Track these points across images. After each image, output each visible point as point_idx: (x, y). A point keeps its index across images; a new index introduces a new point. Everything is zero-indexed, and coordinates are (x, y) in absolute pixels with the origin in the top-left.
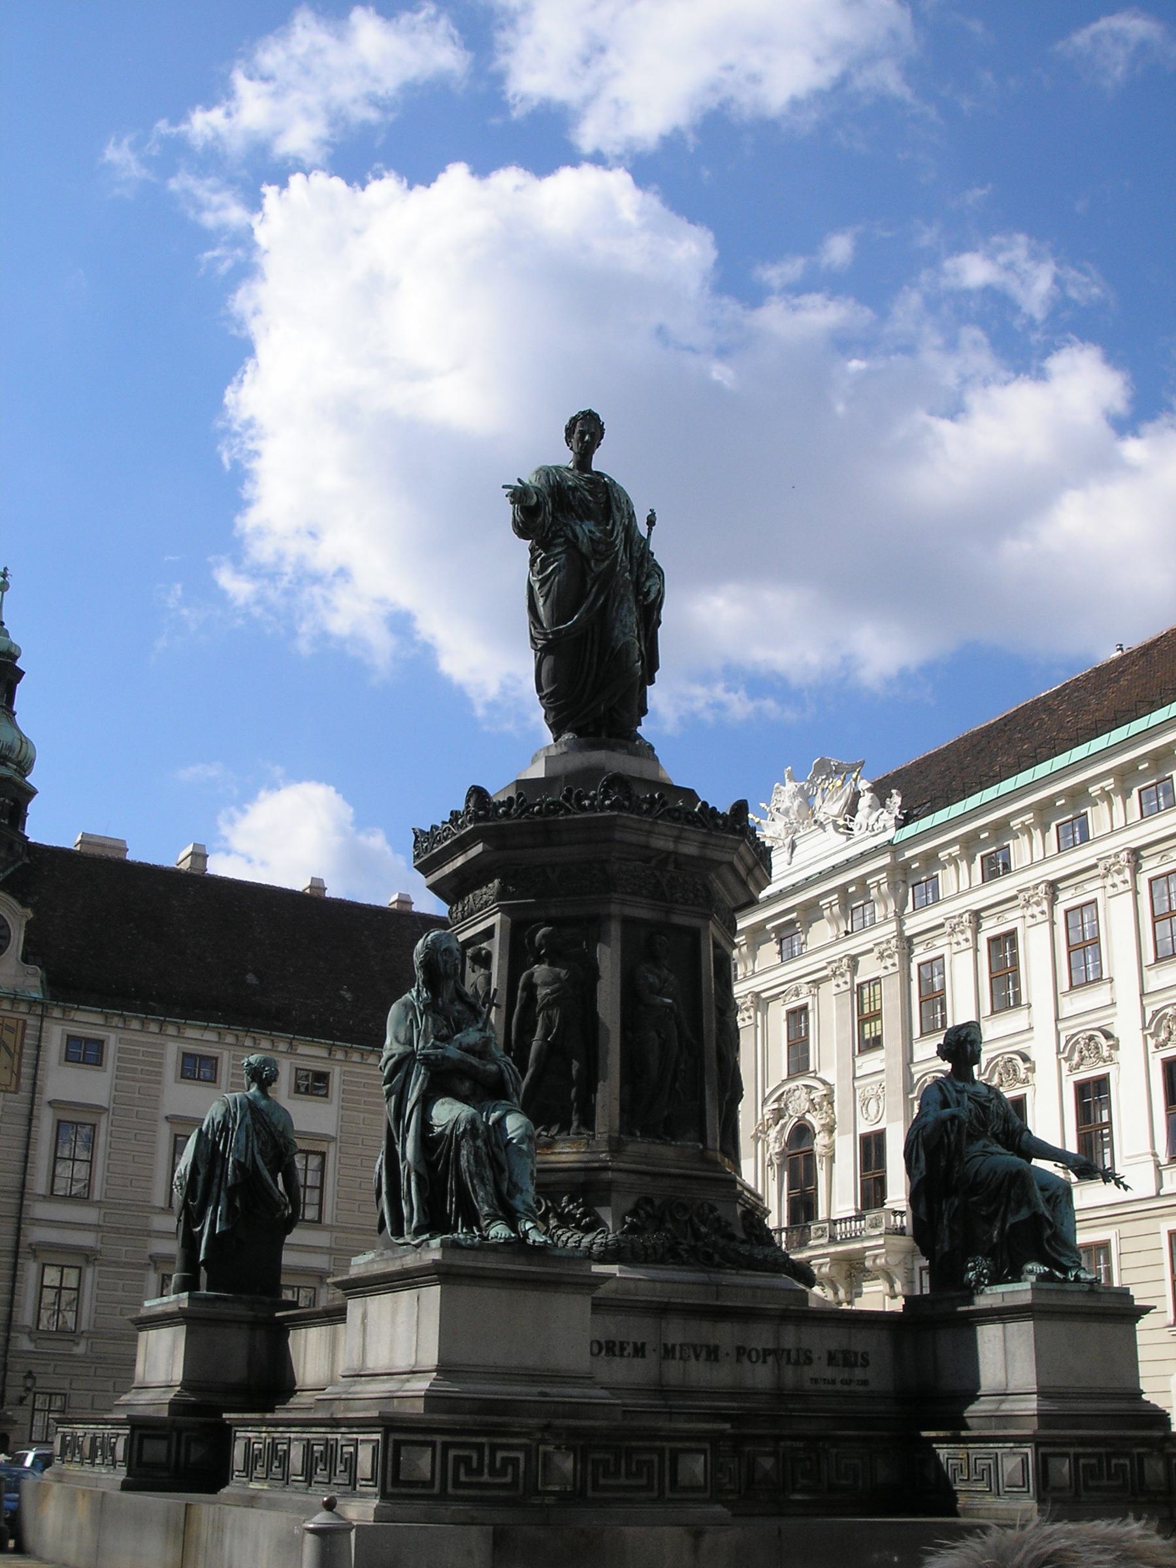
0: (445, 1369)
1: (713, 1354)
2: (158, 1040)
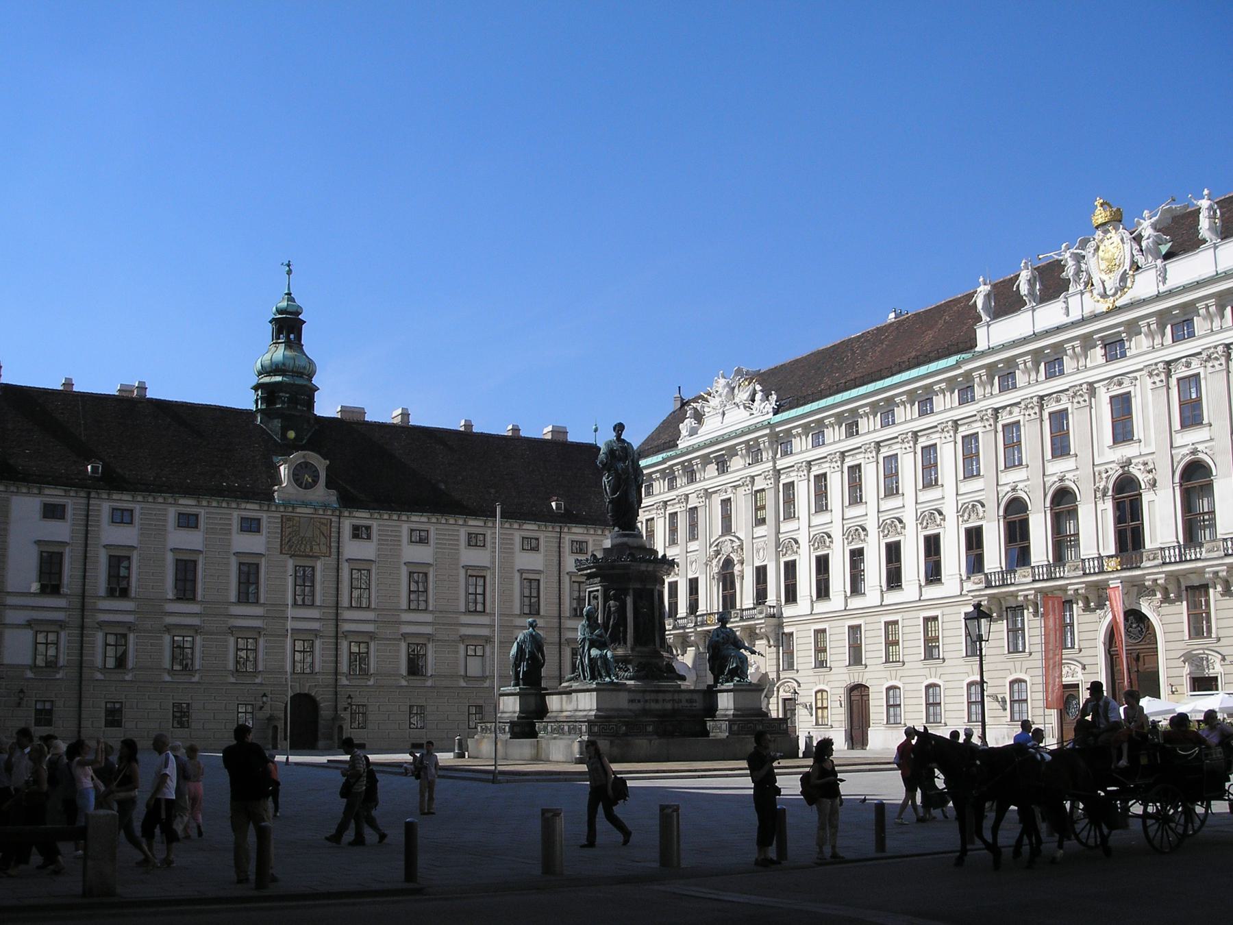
0: (598, 709)
1: (657, 701)
2: (398, 523)
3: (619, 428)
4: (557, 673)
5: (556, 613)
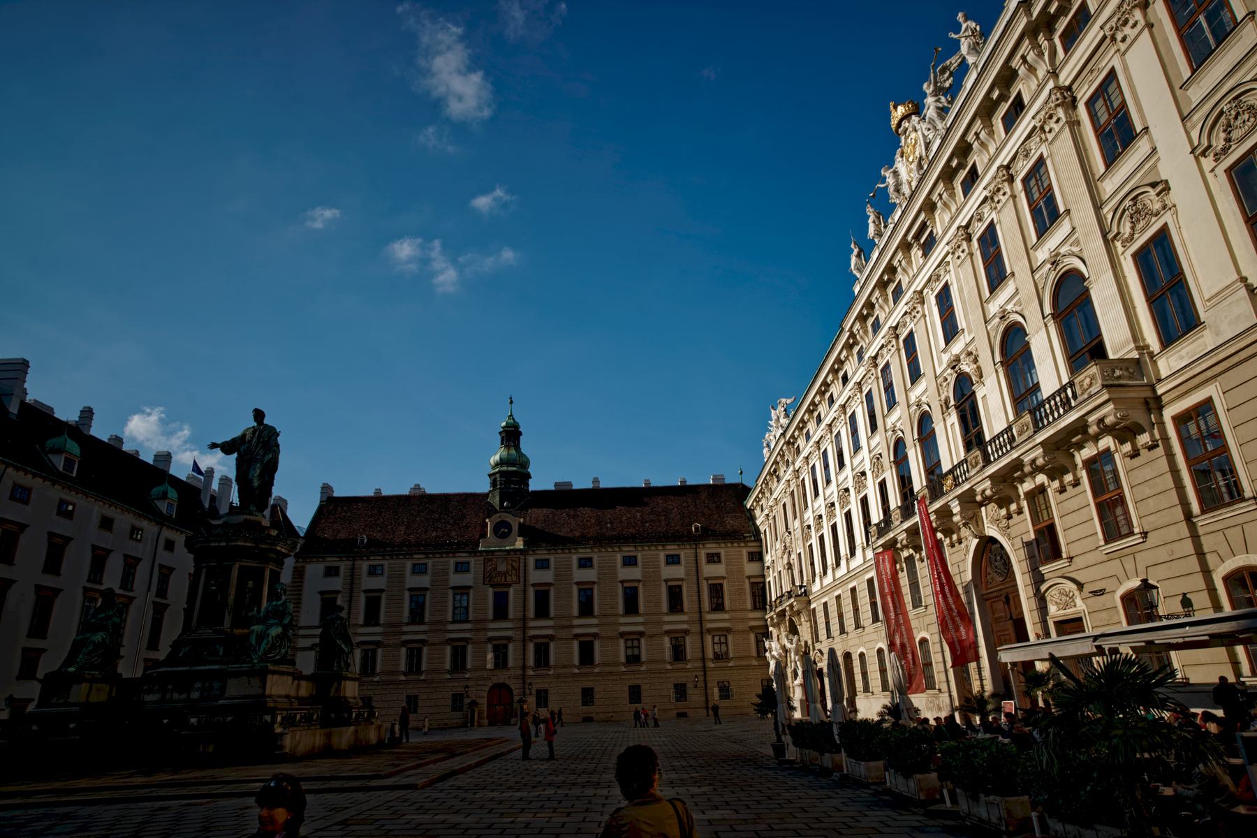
3: (259, 415)
4: (700, 655)
5: (697, 609)
